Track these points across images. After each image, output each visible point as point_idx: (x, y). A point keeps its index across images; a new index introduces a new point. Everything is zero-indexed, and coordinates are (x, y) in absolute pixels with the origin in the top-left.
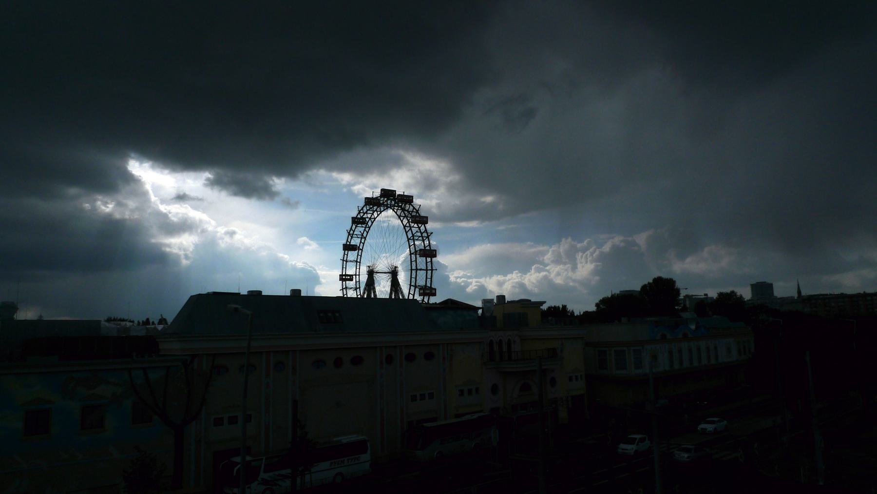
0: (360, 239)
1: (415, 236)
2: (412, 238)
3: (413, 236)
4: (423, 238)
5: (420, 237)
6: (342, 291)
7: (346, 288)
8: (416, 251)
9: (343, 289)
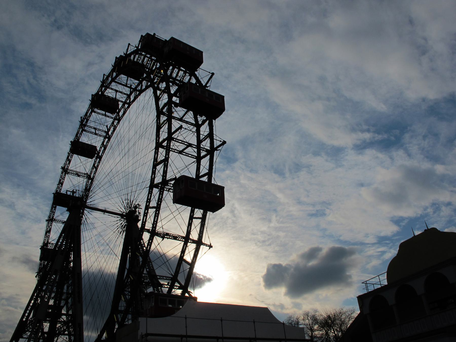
1: (177, 140)
2: (165, 144)
3: (170, 138)
4: (199, 153)
5: (190, 145)
8: (165, 182)
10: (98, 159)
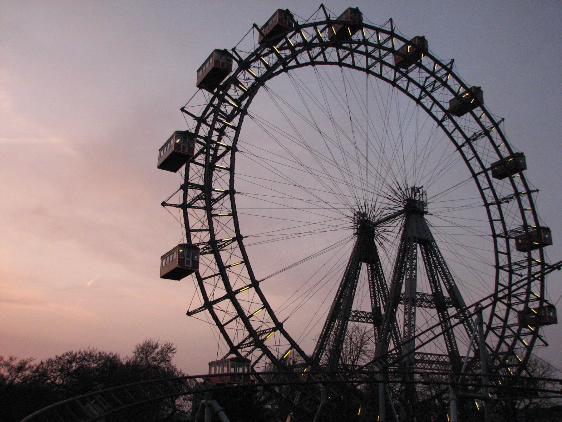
0: (514, 259)
6: (497, 120)
7: (487, 133)
9: (496, 125)
10: (490, 200)
